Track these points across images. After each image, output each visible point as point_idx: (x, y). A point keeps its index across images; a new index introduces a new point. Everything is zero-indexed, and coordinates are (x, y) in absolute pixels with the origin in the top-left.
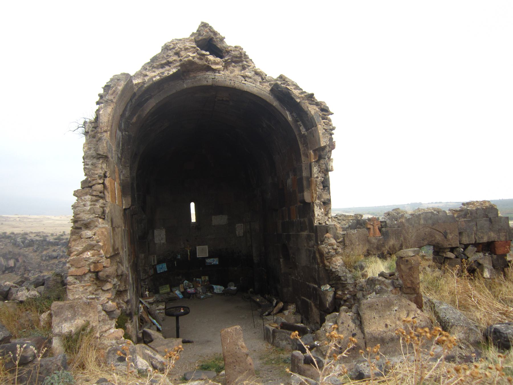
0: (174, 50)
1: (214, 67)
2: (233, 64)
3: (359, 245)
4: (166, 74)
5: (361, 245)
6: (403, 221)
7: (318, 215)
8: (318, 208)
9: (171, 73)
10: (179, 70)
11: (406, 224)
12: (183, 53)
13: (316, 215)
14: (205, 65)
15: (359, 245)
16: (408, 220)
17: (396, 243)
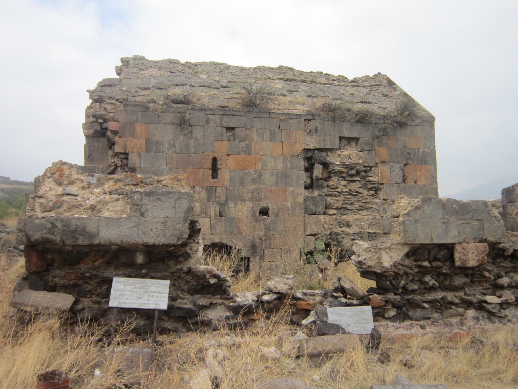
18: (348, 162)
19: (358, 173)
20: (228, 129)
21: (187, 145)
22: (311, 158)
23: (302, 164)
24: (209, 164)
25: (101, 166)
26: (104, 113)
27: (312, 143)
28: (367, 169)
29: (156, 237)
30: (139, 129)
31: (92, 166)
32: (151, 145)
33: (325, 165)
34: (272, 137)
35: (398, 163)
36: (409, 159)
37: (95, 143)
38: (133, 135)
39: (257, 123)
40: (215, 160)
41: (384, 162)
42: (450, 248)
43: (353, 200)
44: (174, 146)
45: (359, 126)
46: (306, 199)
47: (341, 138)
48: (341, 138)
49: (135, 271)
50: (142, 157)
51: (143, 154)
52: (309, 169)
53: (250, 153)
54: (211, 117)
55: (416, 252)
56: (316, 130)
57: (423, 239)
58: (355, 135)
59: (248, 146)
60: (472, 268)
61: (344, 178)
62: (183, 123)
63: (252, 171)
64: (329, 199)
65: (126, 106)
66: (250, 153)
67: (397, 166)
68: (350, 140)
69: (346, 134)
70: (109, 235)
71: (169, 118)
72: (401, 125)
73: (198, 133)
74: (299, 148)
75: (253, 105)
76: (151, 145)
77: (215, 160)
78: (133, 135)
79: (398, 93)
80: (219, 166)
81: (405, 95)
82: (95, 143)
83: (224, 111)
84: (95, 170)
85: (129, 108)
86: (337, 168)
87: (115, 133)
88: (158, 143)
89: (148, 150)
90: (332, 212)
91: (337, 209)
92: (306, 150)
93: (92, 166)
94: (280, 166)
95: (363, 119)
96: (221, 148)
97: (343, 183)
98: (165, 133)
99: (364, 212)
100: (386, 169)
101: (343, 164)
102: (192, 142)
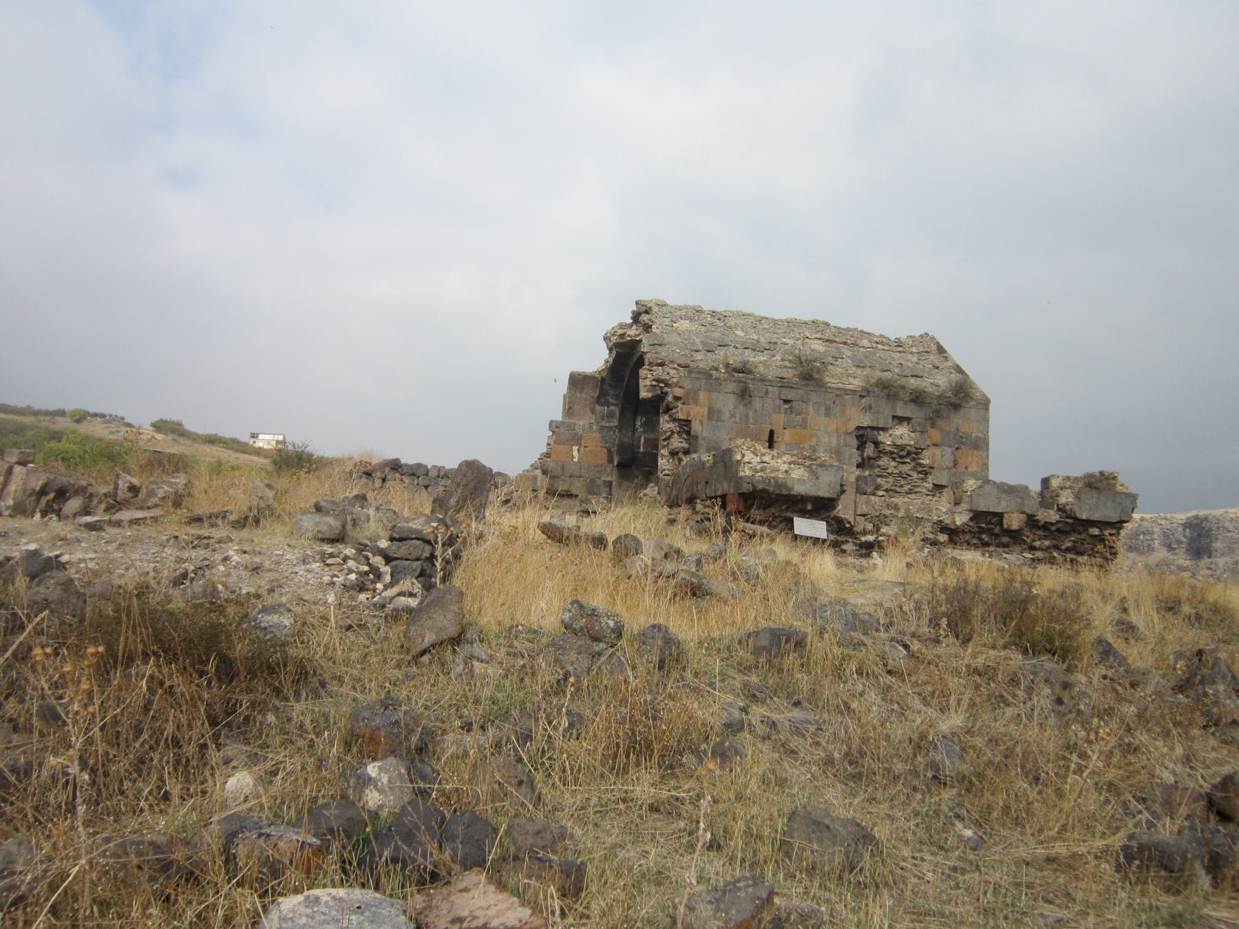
18: (899, 442)
19: (909, 454)
20: (786, 401)
21: (747, 416)
22: (863, 437)
23: (855, 442)
24: (766, 436)
26: (667, 377)
27: (866, 421)
28: (919, 451)
29: (824, 493)
30: (702, 396)
32: (713, 414)
33: (877, 444)
34: (828, 412)
35: (950, 446)
36: (962, 443)
38: (696, 403)
39: (814, 397)
40: (772, 433)
41: (936, 445)
42: (1000, 515)
43: (902, 482)
44: (734, 416)
45: (912, 406)
46: (858, 478)
47: (894, 417)
48: (894, 417)
49: (804, 514)
52: (861, 447)
53: (805, 428)
54: (770, 388)
55: (977, 516)
56: (870, 408)
57: (983, 508)
58: (908, 414)
59: (805, 420)
60: (1015, 531)
61: (894, 459)
62: (744, 394)
63: (807, 446)
64: (879, 480)
65: (690, 372)
66: (805, 428)
67: (949, 450)
68: (900, 420)
69: (899, 413)
70: (799, 489)
71: (731, 387)
72: (956, 407)
73: (757, 404)
74: (852, 426)
75: (809, 375)
76: (713, 414)
77: (772, 433)
78: (696, 403)
79: (950, 364)
80: (775, 439)
81: (959, 370)
83: (783, 383)
85: (693, 375)
86: (889, 448)
87: (677, 399)
88: (720, 412)
89: (710, 418)
90: (881, 493)
91: (886, 490)
92: (859, 428)
94: (834, 442)
95: (918, 398)
96: (778, 420)
97: (893, 464)
98: (727, 402)
99: (913, 496)
100: (938, 452)
101: (894, 444)
102: (751, 413)
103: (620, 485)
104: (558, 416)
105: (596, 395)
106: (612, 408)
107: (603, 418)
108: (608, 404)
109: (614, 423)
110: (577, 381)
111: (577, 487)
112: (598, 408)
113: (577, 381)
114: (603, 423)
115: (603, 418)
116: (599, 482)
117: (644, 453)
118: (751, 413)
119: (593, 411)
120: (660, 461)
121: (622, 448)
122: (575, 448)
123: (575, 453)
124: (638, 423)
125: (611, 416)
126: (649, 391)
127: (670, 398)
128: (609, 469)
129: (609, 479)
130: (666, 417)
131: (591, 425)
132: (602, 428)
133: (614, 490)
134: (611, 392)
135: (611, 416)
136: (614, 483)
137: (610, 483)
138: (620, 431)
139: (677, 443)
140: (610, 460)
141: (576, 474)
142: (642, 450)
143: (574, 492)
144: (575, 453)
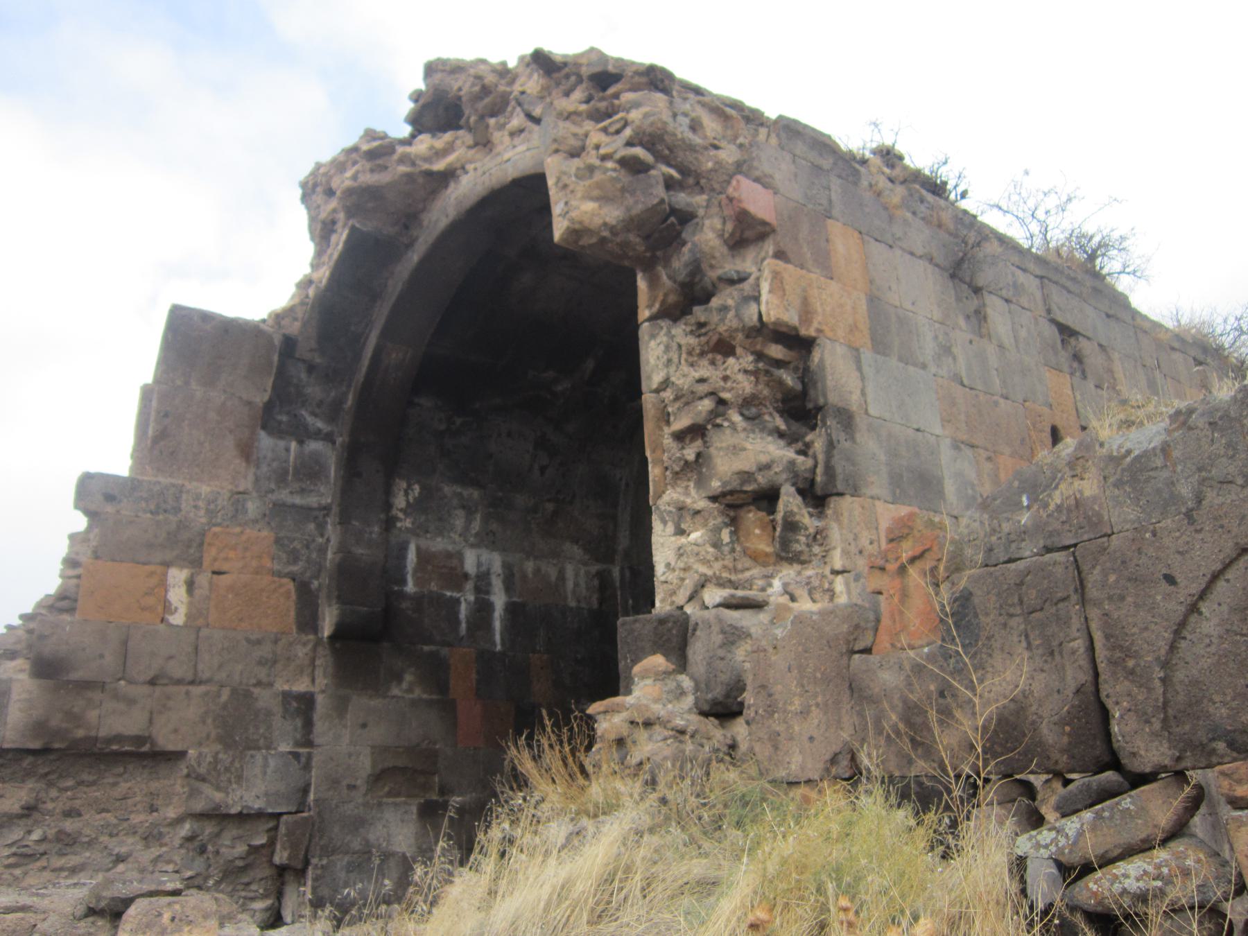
0: (319, 189)
1: (439, 166)
2: (492, 121)
3: (804, 713)
4: (336, 256)
5: (816, 715)
6: (1089, 487)
7: (668, 565)
8: (670, 528)
9: (340, 247)
10: (353, 229)
11: (1122, 515)
12: (335, 184)
13: (659, 569)
14: (409, 177)
15: (804, 713)
16: (1132, 473)
17: (1038, 688)
25: (205, 489)
31: (164, 480)
37: (194, 385)
50: (866, 369)
51: (867, 355)
82: (194, 385)
84: (178, 499)
93: (164, 480)
103: (341, 707)
104: (116, 456)
105: (261, 398)
106: (314, 446)
107: (281, 478)
108: (301, 433)
109: (325, 494)
110: (195, 342)
111: (181, 723)
112: (265, 441)
113: (195, 342)
114: (284, 495)
115: (281, 478)
116: (265, 699)
117: (418, 599)
118: (991, 349)
119: (246, 451)
120: (665, 547)
121: (349, 577)
122: (178, 576)
123: (177, 595)
124: (400, 502)
125: (309, 472)
126: (604, 199)
127: (708, 235)
128: (301, 652)
129: (301, 686)
130: (680, 332)
131: (238, 497)
132: (280, 508)
133: (320, 726)
134: (314, 391)
135: (309, 472)
136: (320, 699)
137: (305, 703)
138: (344, 520)
139: (750, 450)
140: (308, 621)
141: (177, 670)
142: (410, 587)
143: (167, 742)
144: (177, 595)
